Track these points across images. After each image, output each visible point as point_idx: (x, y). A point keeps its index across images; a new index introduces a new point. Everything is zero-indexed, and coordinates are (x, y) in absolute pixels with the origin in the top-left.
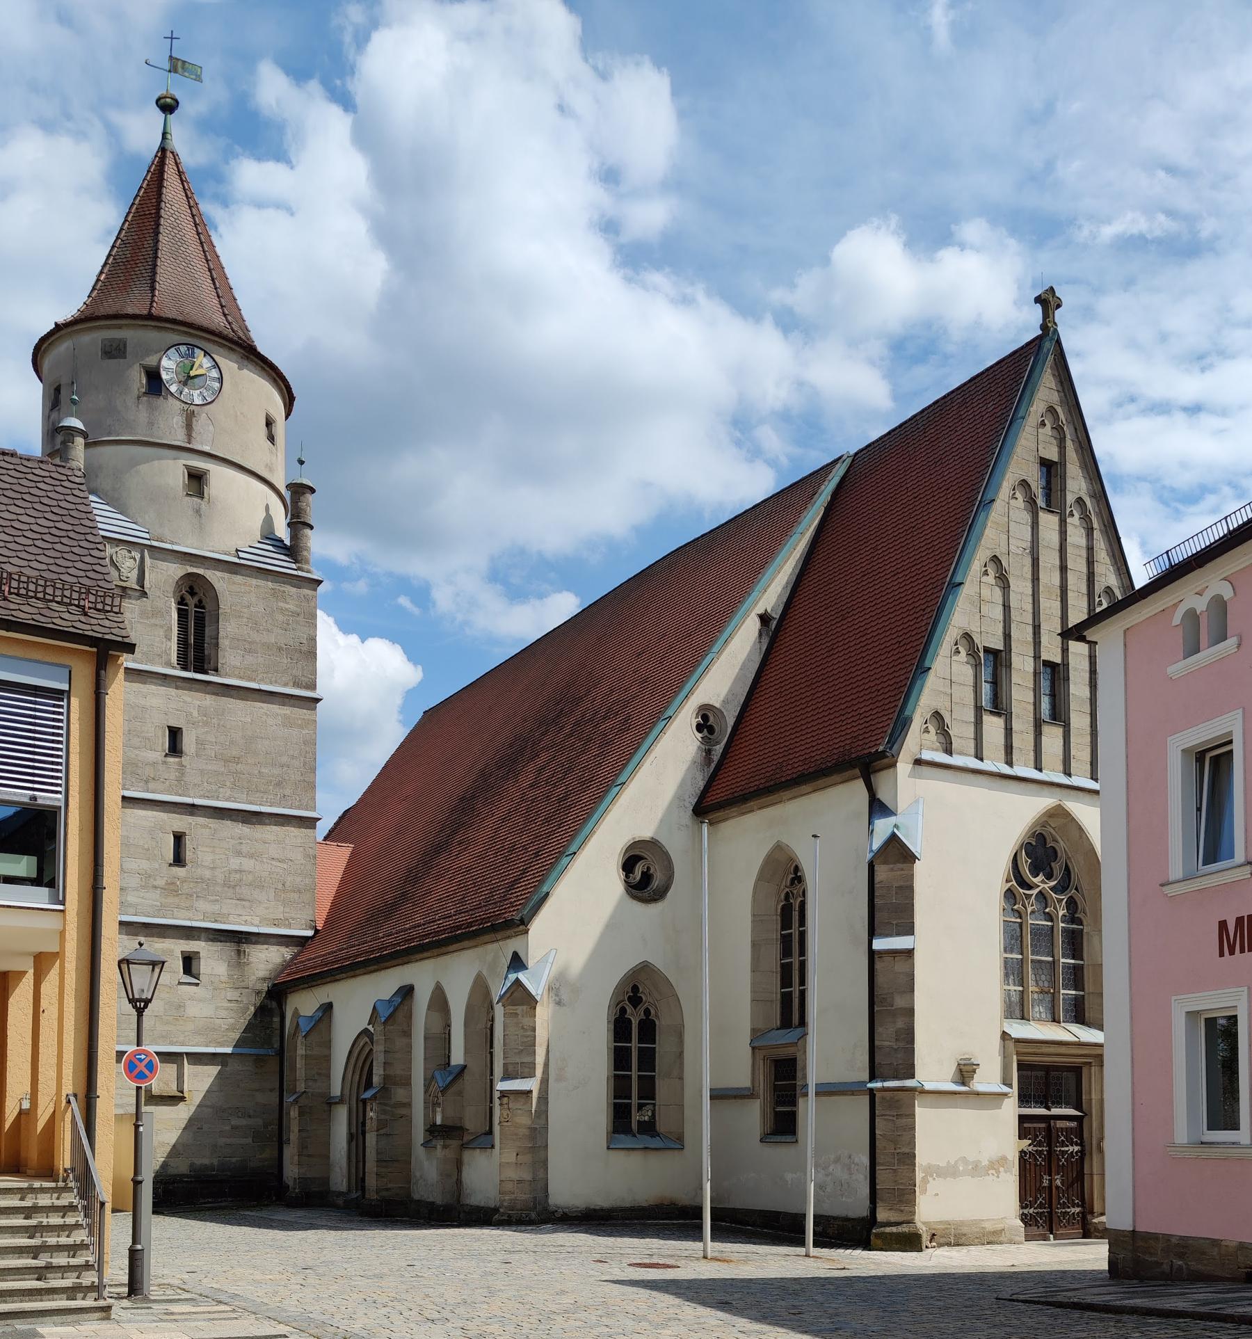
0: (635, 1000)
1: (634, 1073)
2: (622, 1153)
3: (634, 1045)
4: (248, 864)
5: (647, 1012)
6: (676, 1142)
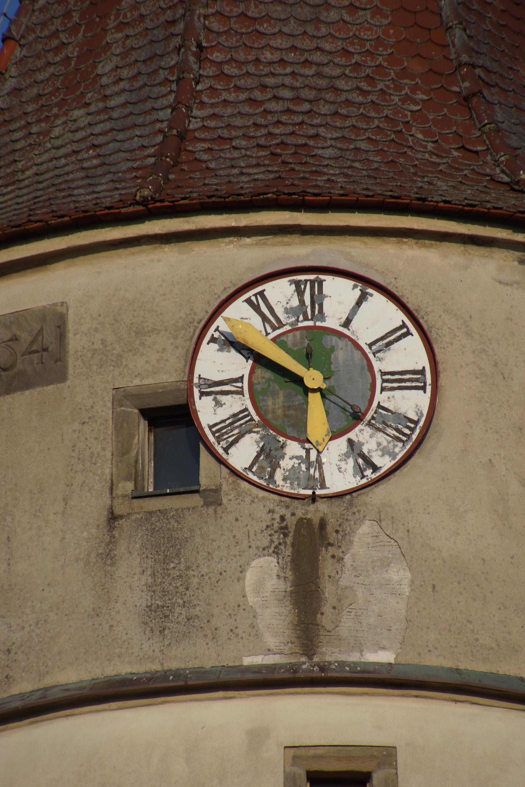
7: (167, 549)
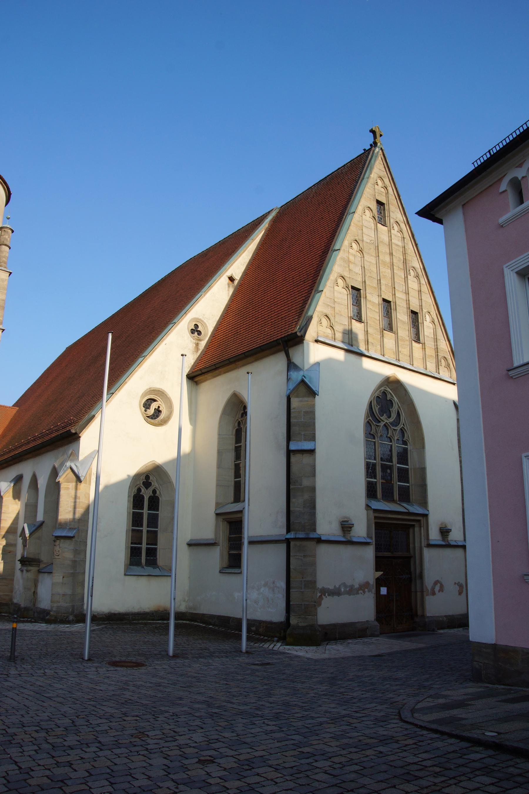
0: (147, 484)
1: (145, 529)
2: (135, 578)
3: (145, 511)
5: (154, 492)
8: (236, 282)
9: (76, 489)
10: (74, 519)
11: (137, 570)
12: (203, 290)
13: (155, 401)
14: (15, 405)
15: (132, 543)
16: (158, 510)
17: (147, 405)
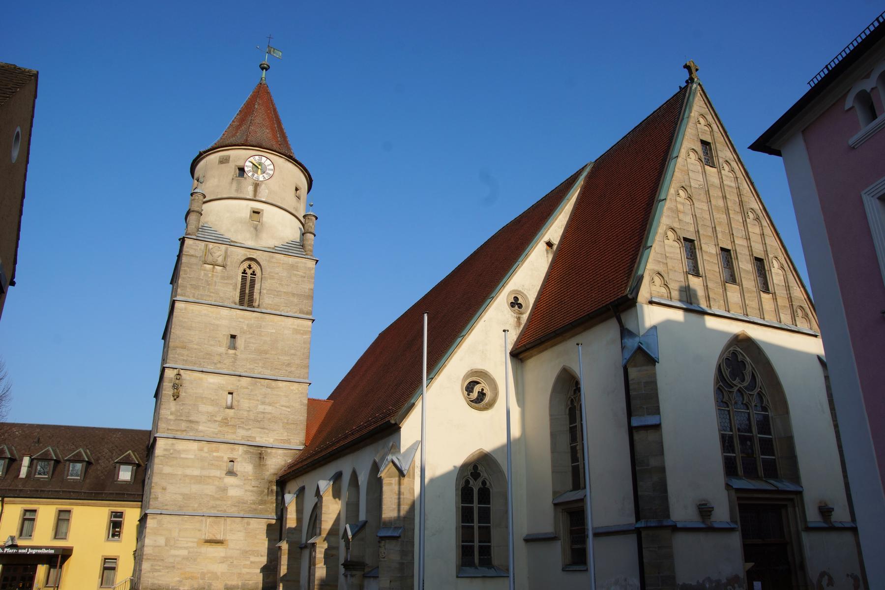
0: (476, 475)
1: (476, 525)
3: (476, 505)
4: (269, 409)
5: (484, 483)
6: (503, 572)
7: (239, 183)
8: (555, 247)
9: (400, 484)
10: (399, 517)
11: (470, 571)
12: (520, 259)
13: (478, 383)
14: (330, 398)
15: (463, 541)
16: (489, 503)
17: (469, 388)
